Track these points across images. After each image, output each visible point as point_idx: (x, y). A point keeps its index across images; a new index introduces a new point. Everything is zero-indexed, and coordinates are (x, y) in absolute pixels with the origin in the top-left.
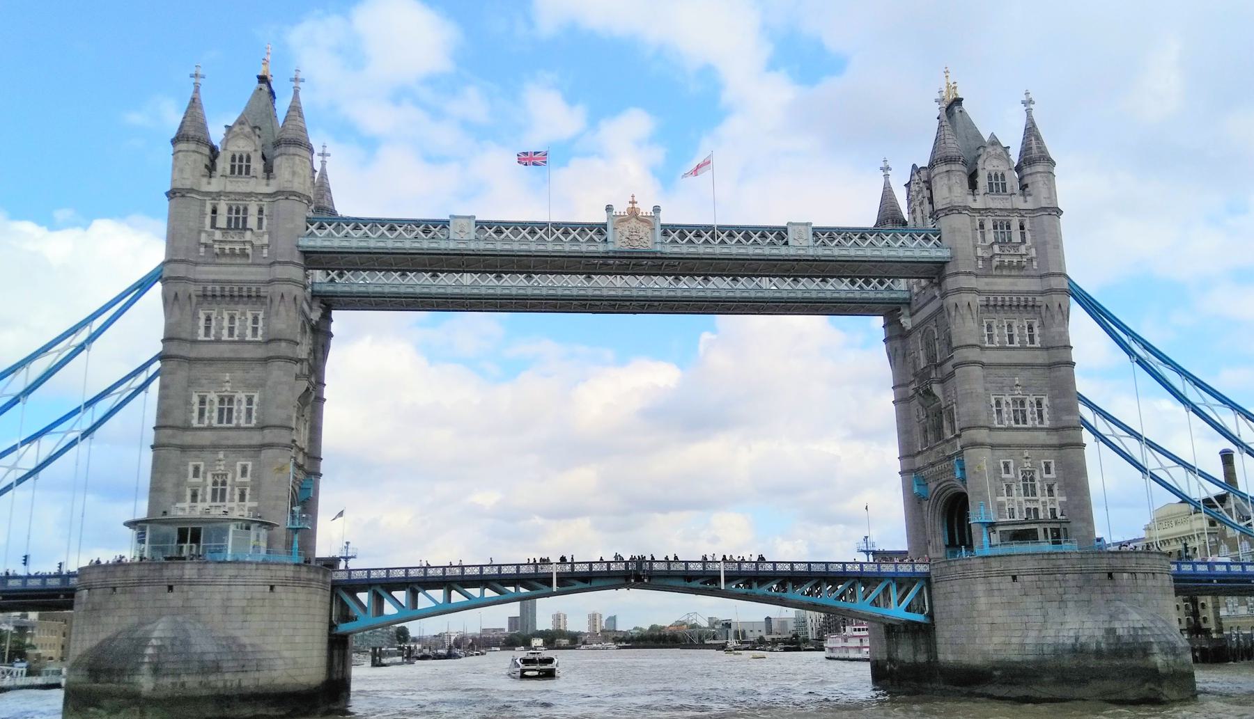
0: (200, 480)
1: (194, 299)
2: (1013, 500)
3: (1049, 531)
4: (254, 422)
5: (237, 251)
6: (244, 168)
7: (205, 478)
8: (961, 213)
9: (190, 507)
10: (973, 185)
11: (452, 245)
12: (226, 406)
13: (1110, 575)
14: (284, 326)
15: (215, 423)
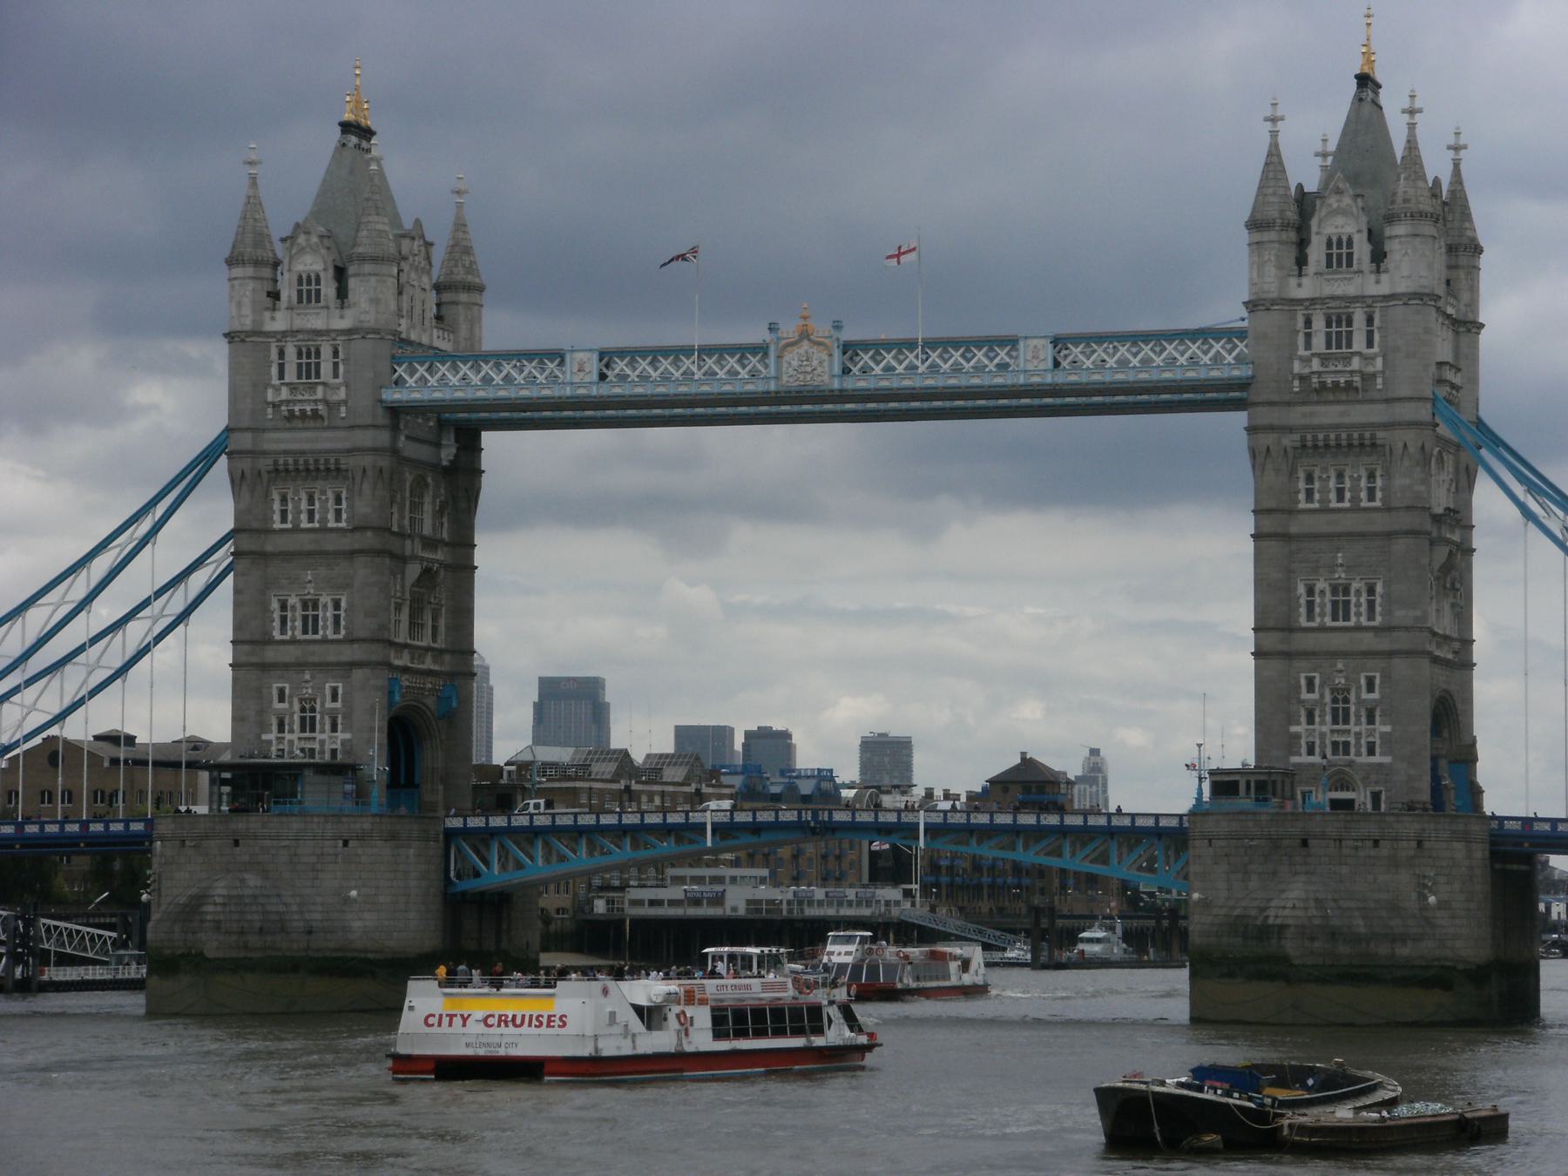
0: (285, 705)
1: (265, 477)
2: (1314, 730)
3: (1252, 785)
4: (343, 632)
5: (309, 413)
6: (313, 292)
7: (291, 703)
8: (1268, 309)
9: (278, 738)
10: (1301, 261)
11: (568, 391)
12: (310, 613)
13: (1305, 843)
14: (369, 510)
15: (299, 635)
